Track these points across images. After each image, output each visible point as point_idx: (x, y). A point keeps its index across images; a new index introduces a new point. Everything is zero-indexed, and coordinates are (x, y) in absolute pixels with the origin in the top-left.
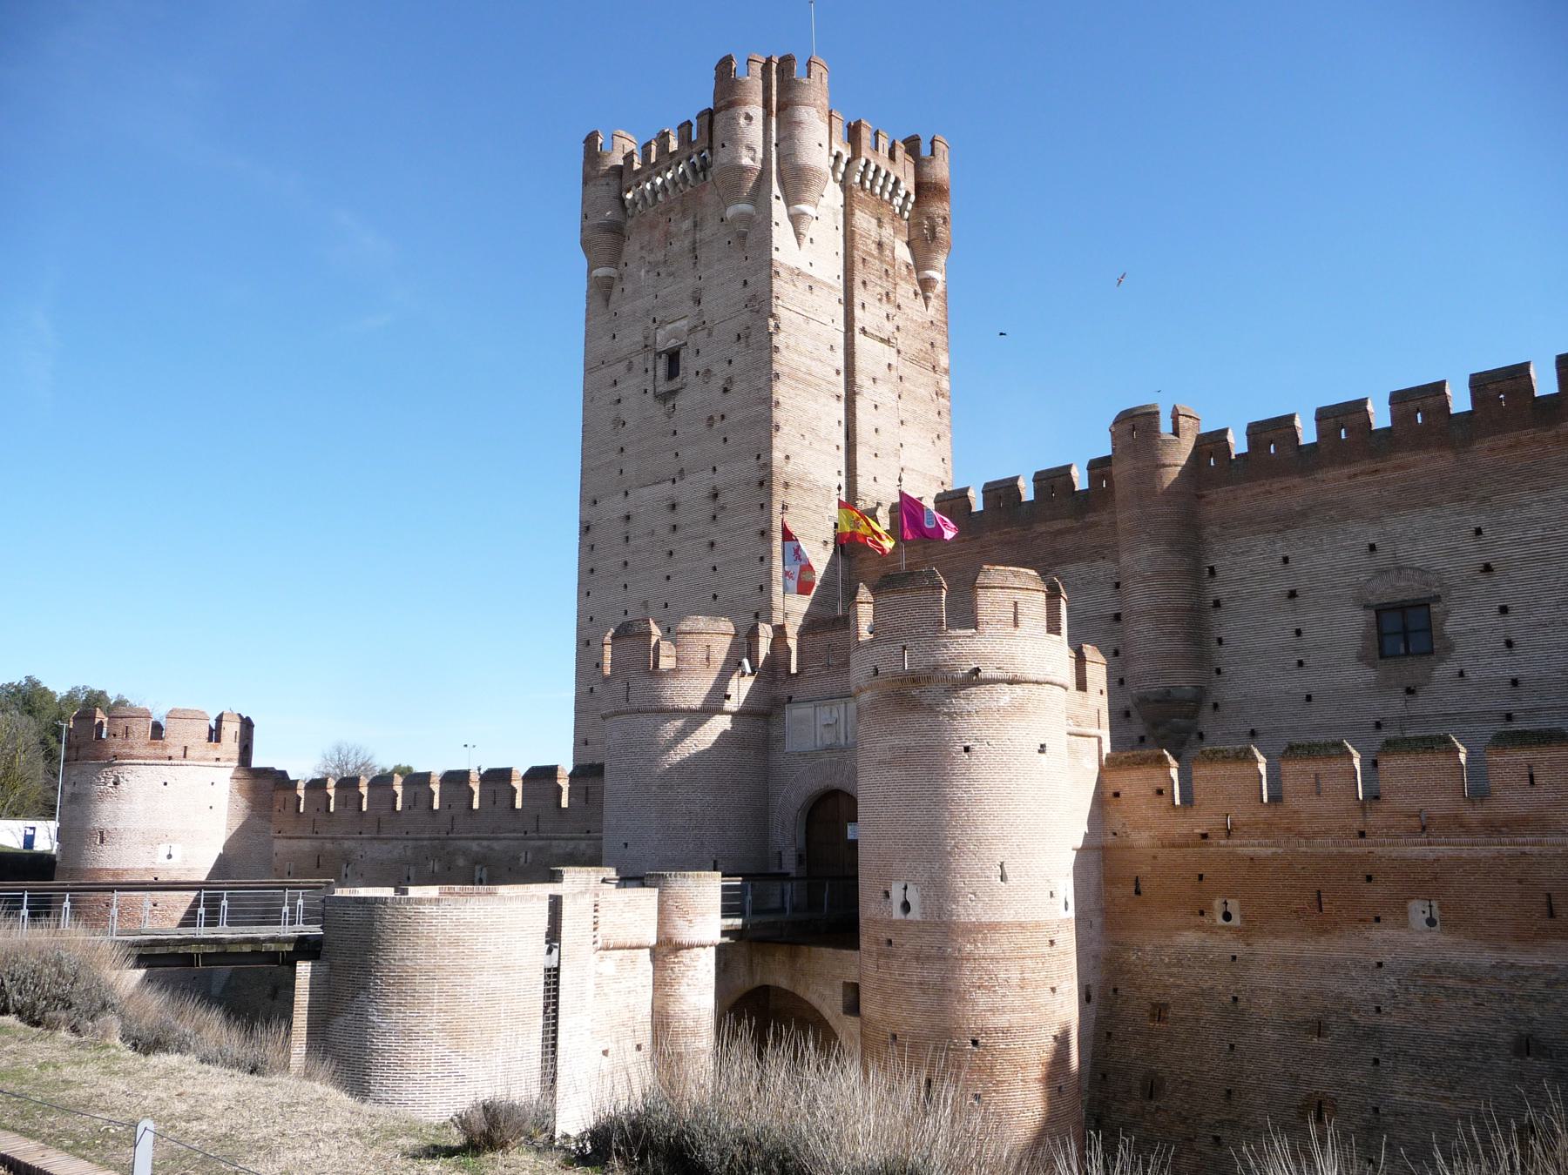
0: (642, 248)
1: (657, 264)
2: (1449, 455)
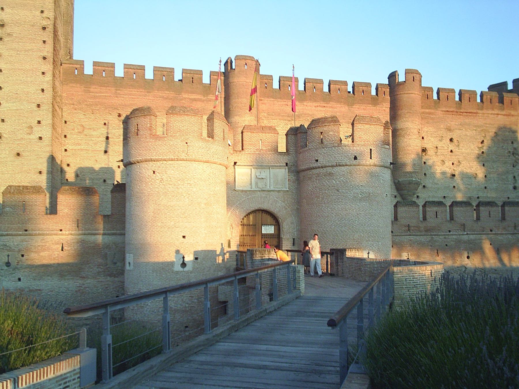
2: (347, 107)
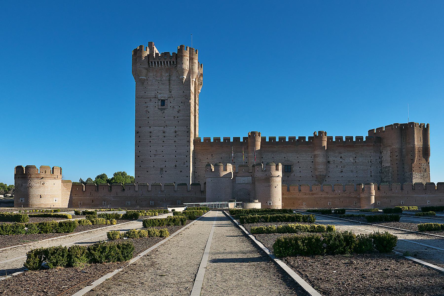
0: (154, 75)
1: (158, 80)
